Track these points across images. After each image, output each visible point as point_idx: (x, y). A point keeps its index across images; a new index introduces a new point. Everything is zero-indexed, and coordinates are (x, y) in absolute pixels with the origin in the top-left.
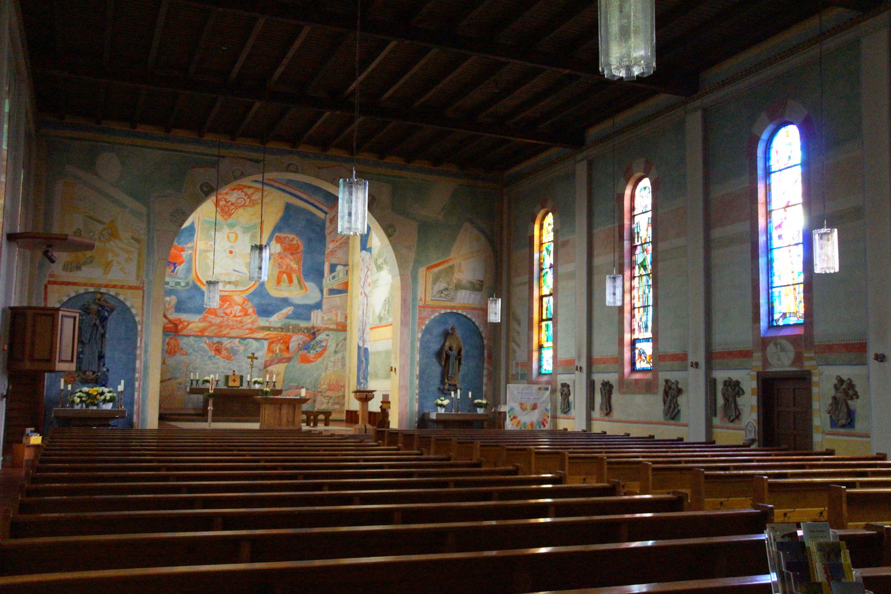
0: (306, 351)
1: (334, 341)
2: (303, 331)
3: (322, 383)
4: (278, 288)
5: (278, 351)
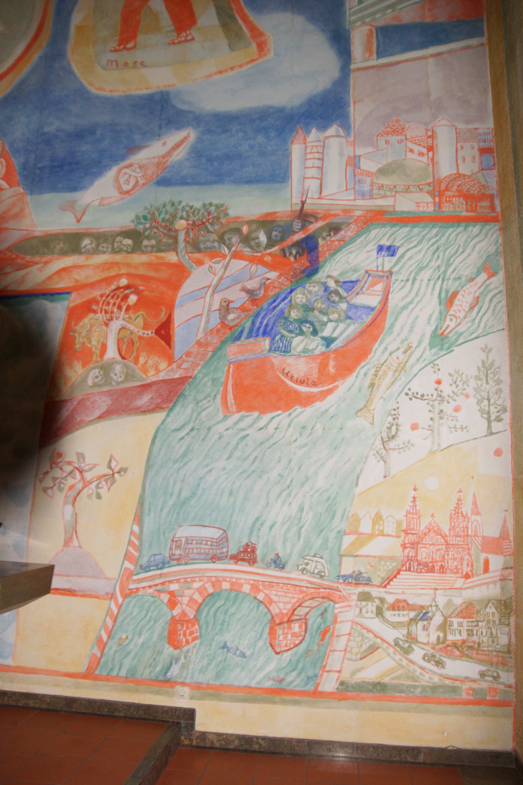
0: (266, 343)
1: (425, 275)
2: (246, 240)
3: (366, 527)
4: (124, 56)
5: (112, 353)
